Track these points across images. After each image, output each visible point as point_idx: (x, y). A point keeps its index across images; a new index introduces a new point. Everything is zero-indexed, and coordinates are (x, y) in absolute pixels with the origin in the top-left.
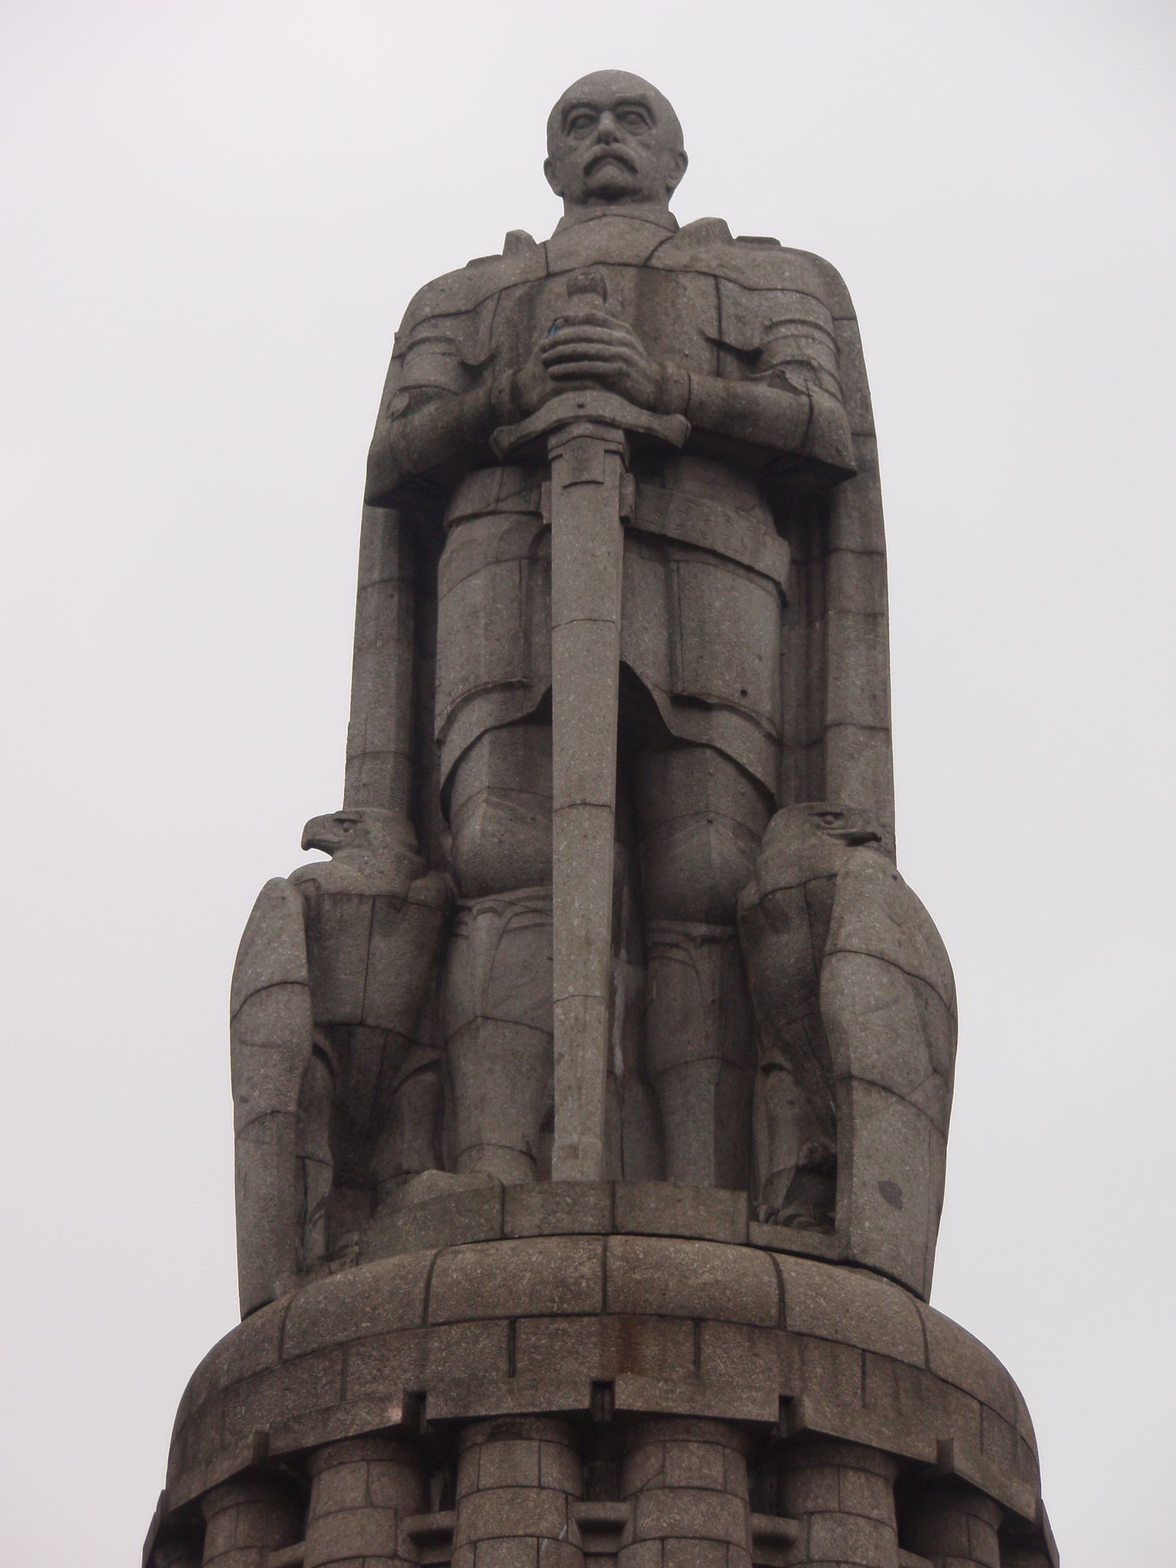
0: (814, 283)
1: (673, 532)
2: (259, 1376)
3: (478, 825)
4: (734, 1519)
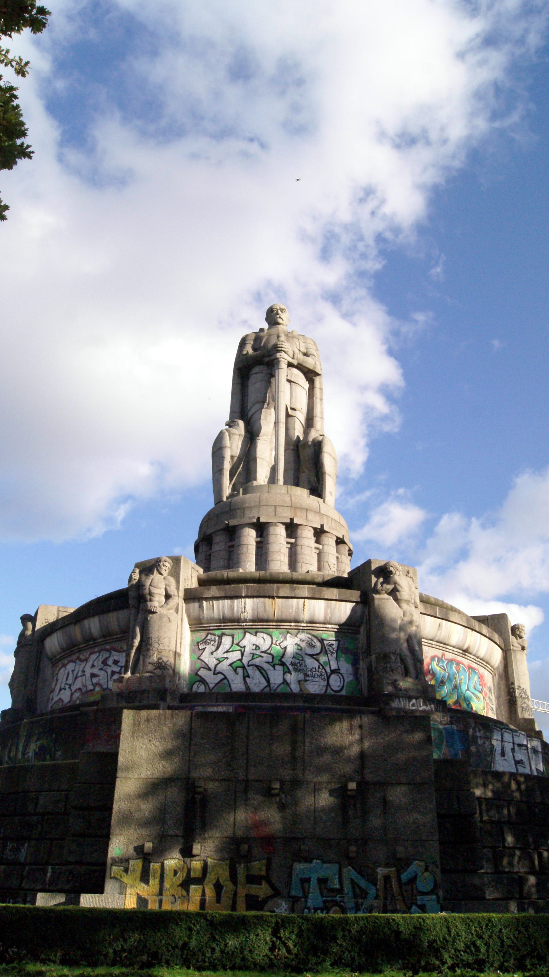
0: (313, 343)
1: (292, 380)
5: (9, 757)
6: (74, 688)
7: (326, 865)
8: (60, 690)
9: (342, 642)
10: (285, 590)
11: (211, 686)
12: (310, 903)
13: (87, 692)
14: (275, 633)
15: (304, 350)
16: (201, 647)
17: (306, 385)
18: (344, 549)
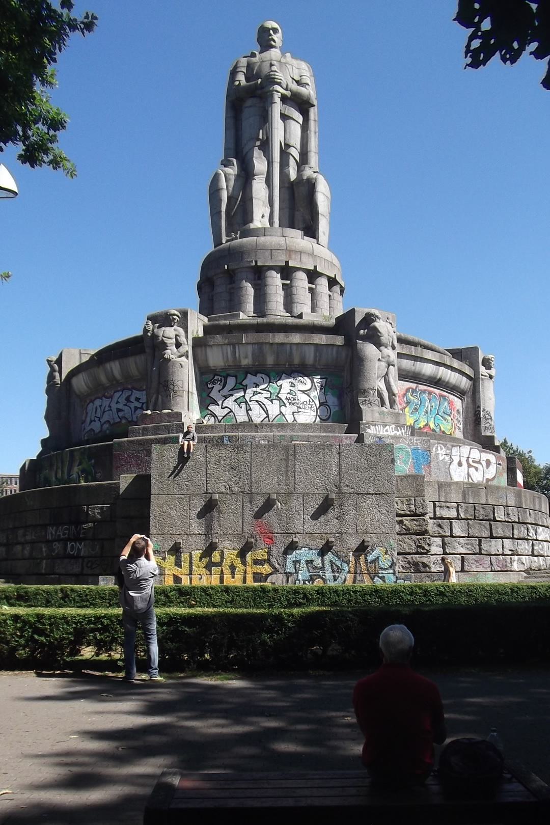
4: (307, 285)
5: (56, 478)
6: (103, 420)
8: (91, 421)
11: (220, 418)
12: (300, 577)
13: (115, 424)
15: (297, 78)
16: (210, 386)
18: (337, 288)
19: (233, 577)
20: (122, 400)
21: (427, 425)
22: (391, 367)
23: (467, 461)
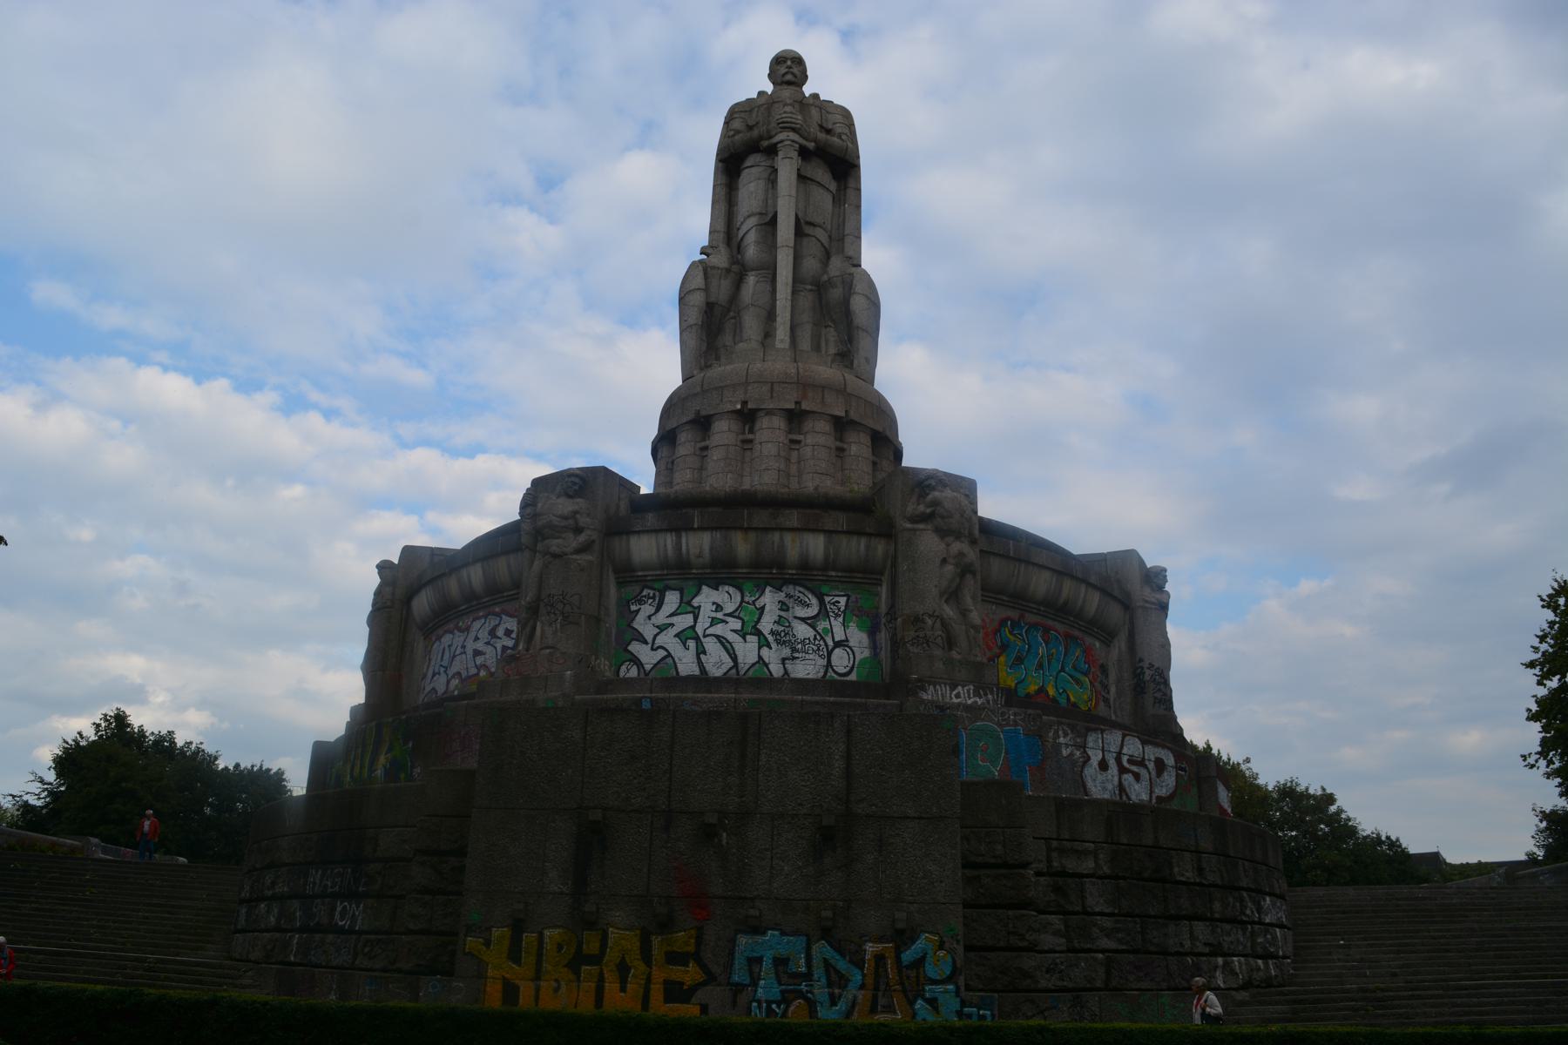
2: (696, 395)
3: (752, 252)
7: (786, 939)
9: (853, 598)
10: (761, 517)
11: (648, 667)
13: (469, 677)
14: (748, 586)
16: (633, 608)
17: (833, 186)
19: (623, 989)
20: (484, 635)
21: (1042, 690)
22: (969, 576)
23: (1118, 760)
